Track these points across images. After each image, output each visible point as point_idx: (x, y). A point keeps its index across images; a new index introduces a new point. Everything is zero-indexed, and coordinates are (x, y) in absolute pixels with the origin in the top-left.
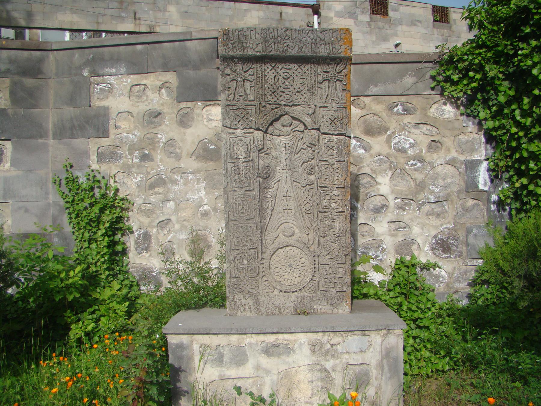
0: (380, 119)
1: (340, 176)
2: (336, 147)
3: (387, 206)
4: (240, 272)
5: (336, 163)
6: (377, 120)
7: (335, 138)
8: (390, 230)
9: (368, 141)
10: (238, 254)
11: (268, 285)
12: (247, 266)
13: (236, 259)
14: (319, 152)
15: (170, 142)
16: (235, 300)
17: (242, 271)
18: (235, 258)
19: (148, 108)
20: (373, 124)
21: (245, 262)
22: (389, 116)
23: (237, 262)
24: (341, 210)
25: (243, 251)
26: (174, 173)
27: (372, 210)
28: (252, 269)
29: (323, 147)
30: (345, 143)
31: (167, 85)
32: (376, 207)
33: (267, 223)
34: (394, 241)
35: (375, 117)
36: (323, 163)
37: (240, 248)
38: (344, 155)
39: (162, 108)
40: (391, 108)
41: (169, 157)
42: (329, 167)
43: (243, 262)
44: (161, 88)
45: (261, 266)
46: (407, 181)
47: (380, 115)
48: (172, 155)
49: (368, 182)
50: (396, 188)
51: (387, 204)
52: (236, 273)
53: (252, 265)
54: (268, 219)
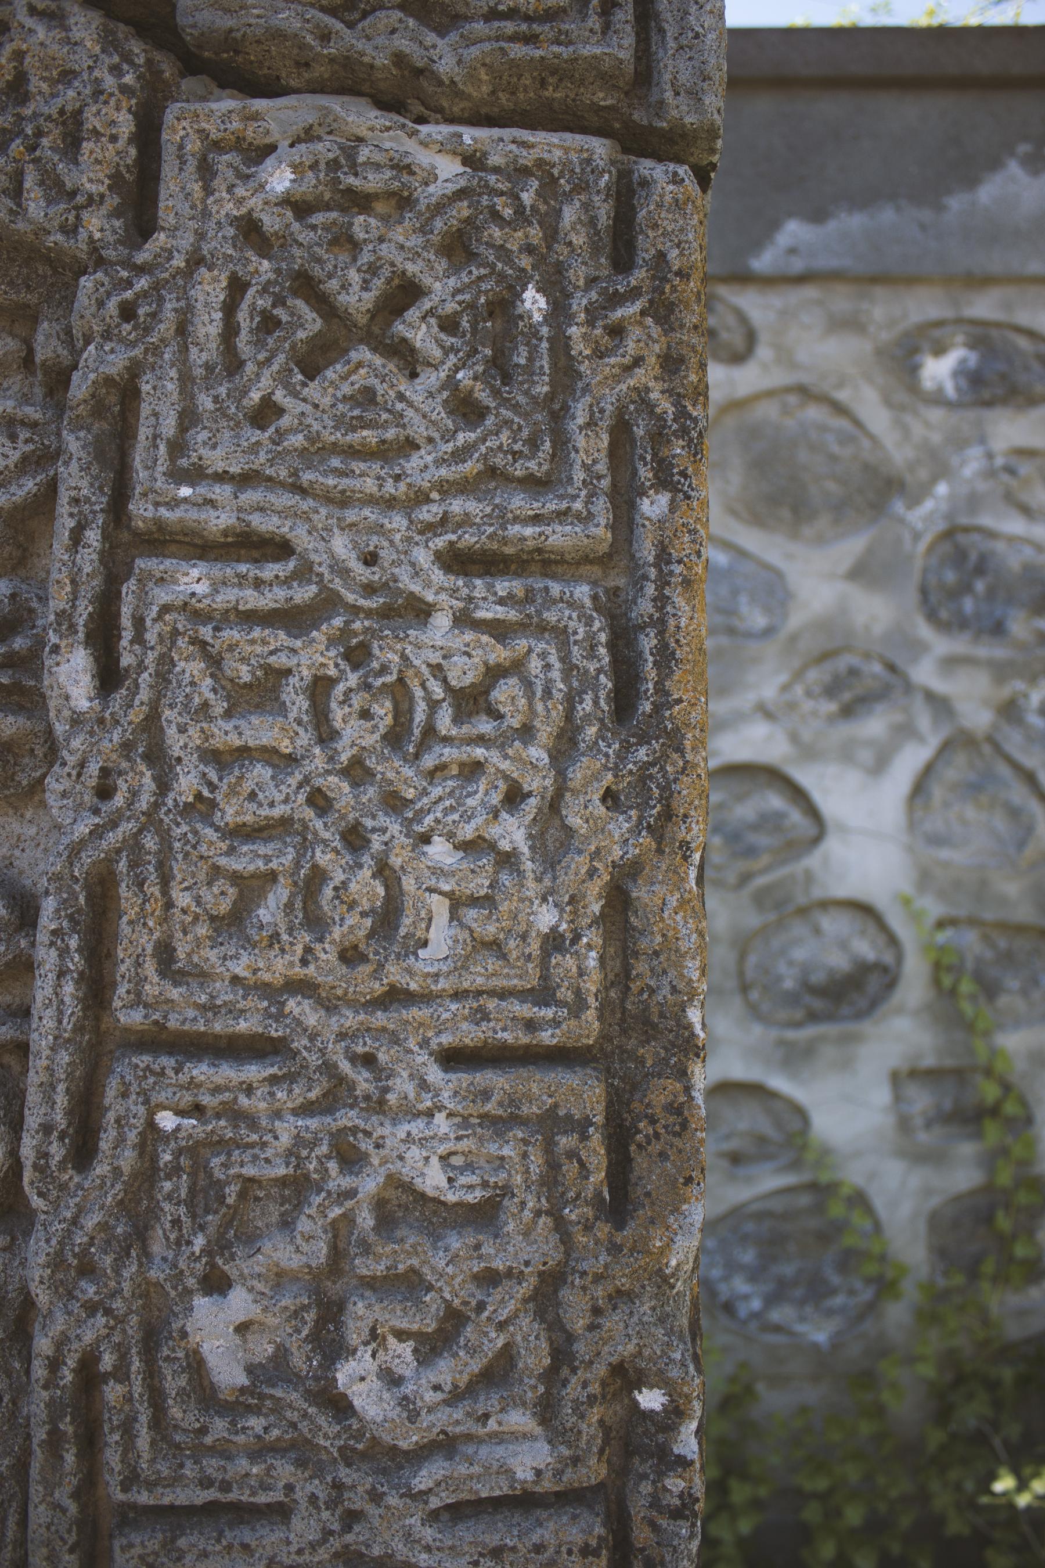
0: (842, 423)
1: (513, 832)
2: (442, 289)
3: (885, 969)
5: (435, 585)
6: (823, 428)
7: (437, 161)
8: (904, 1124)
9: (773, 557)
14: (126, 392)
20: (803, 456)
22: (902, 408)
24: (530, 1460)
27: (792, 999)
29: (210, 290)
30: (621, 244)
32: (818, 978)
34: (927, 1192)
35: (814, 413)
36: (194, 580)
38: (590, 448)
40: (903, 358)
42: (313, 655)
46: (1014, 813)
47: (843, 395)
49: (770, 822)
50: (945, 854)
51: (888, 958)
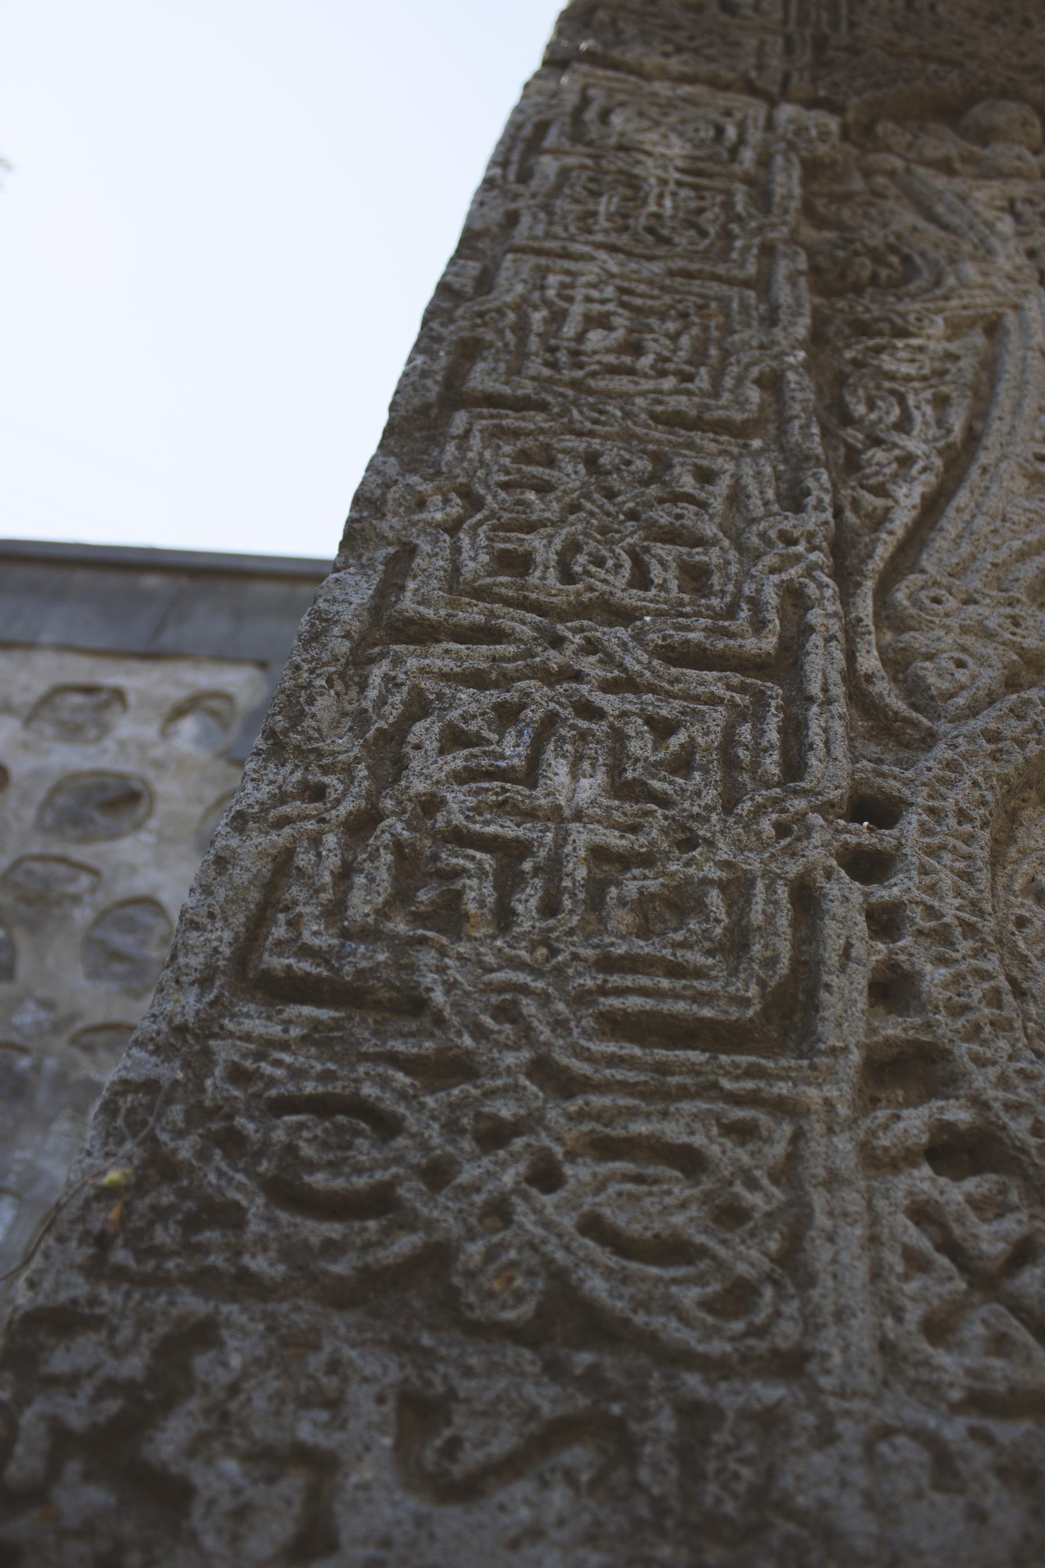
4: (449, 916)
10: (477, 680)
11: (990, 1239)
12: (581, 837)
13: (425, 732)
15: (131, 911)
16: (169, 1441)
17: (477, 894)
18: (419, 707)
19: (87, 765)
21: (573, 784)
23: (428, 769)
25: (555, 659)
26: (89, 1049)
28: (683, 902)
31: (216, 704)
33: (902, 519)
37: (522, 625)
39: (151, 774)
41: (94, 974)
43: (532, 772)
44: (180, 712)
45: (845, 898)
48: (118, 968)
52: (361, 905)
53: (689, 843)
54: (908, 498)
